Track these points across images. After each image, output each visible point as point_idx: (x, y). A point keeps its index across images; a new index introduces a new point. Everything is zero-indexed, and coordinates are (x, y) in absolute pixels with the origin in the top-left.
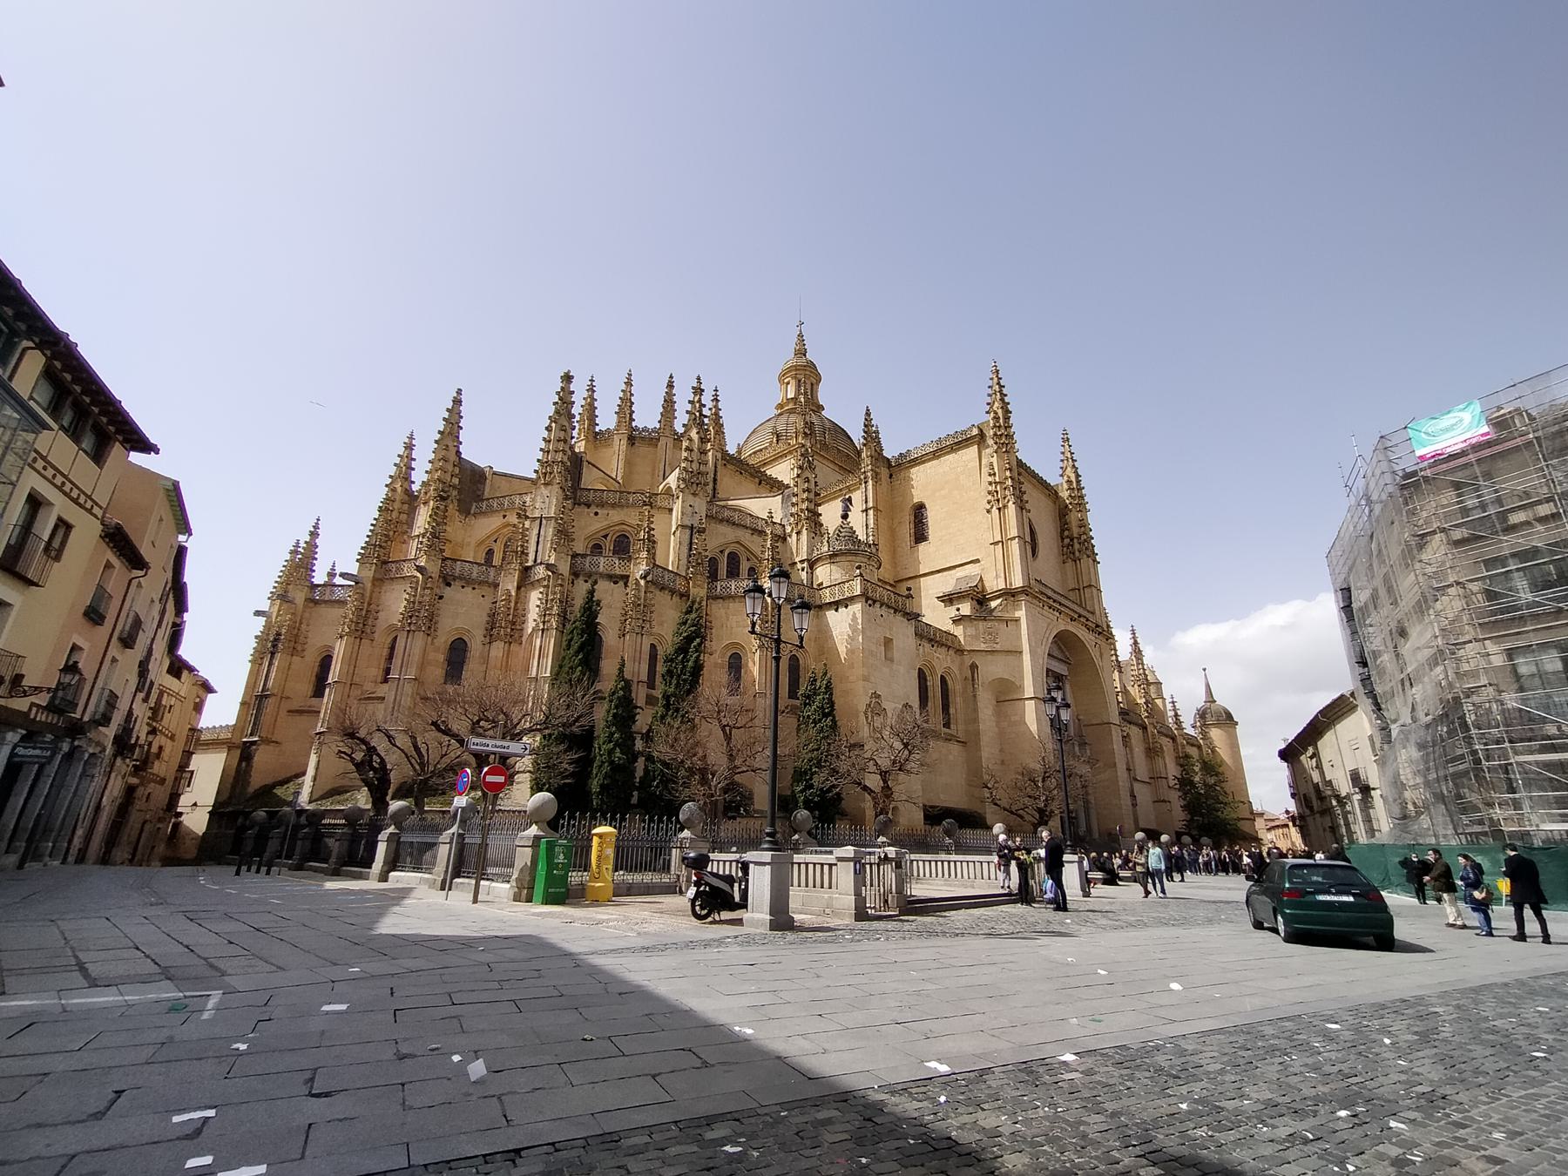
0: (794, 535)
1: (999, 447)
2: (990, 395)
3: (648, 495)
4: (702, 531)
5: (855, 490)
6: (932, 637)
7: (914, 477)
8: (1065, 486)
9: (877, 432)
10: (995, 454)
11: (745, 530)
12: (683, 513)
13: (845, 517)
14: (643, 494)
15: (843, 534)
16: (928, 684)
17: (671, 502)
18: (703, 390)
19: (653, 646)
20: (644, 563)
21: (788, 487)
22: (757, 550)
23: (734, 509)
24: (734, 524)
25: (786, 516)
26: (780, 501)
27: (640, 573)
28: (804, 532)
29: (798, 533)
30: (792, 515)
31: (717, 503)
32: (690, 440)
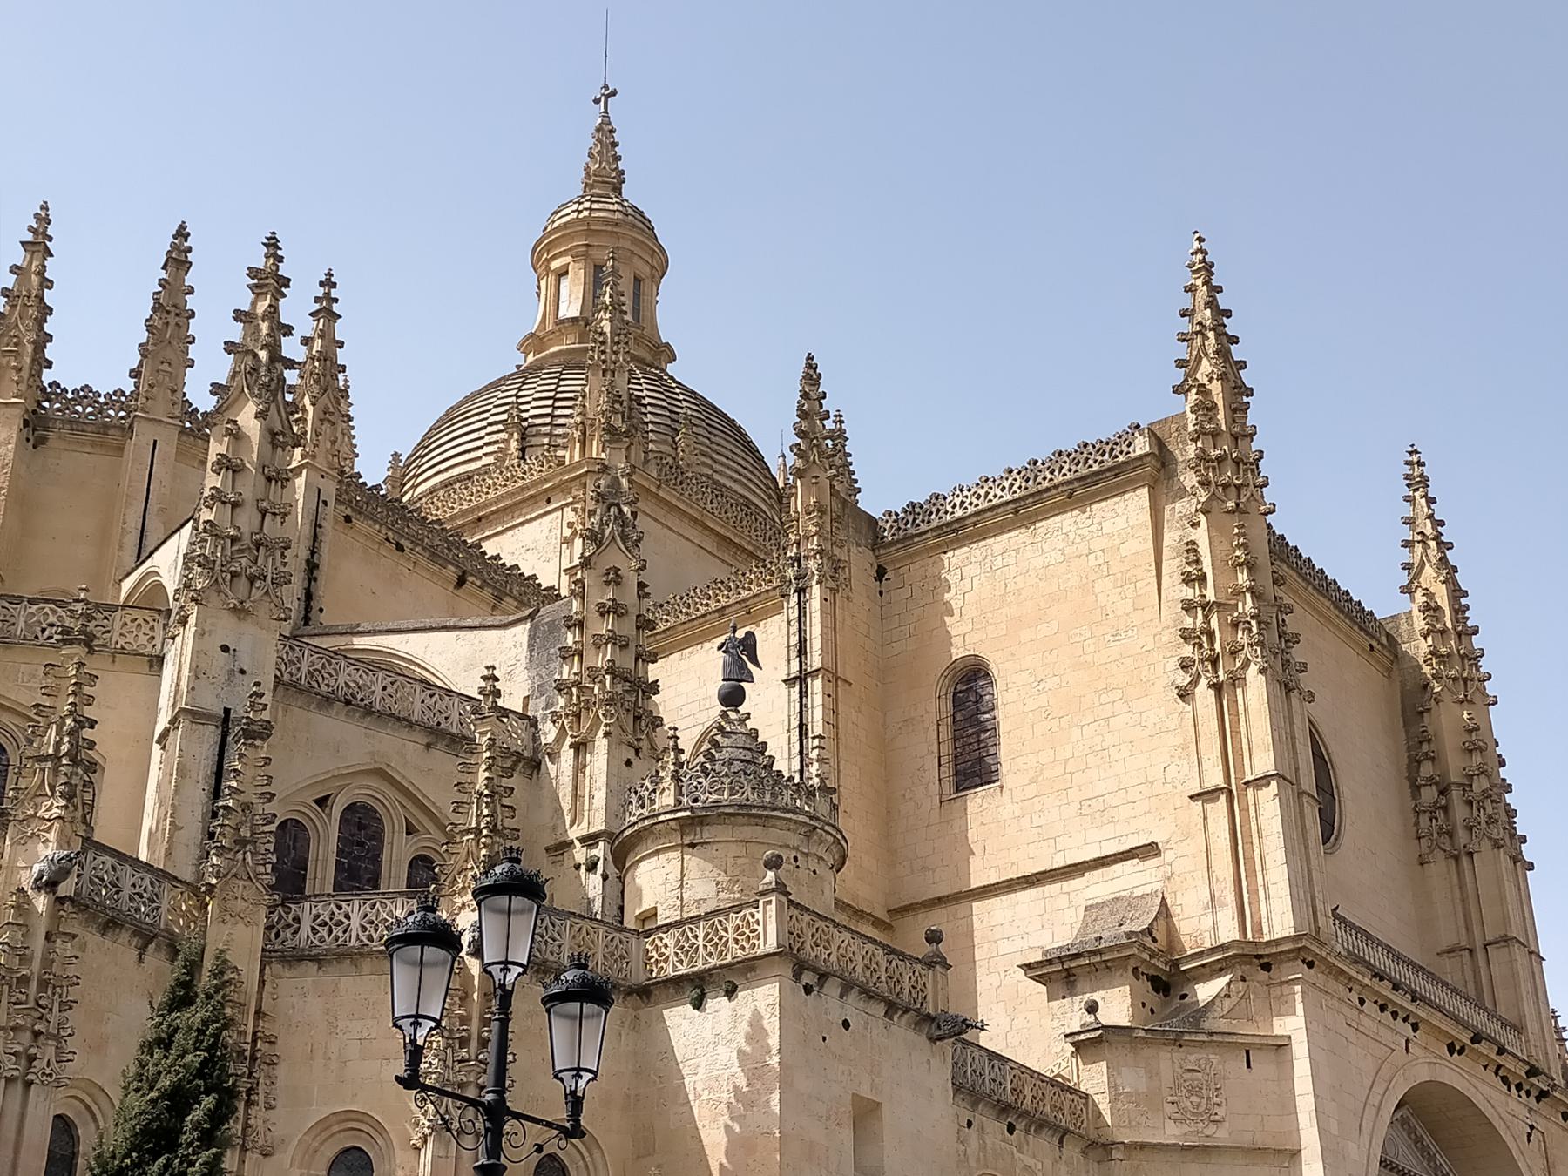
0: (567, 754)
1: (1213, 497)
2: (1183, 338)
3: (79, 608)
4: (258, 733)
5: (767, 614)
7: (952, 579)
8: (1420, 623)
9: (839, 436)
10: (1202, 518)
11: (404, 733)
12: (196, 672)
13: (732, 697)
14: (62, 604)
15: (725, 754)
17: (159, 633)
18: (286, 282)
19: (63, 1127)
20: (52, 836)
21: (552, 595)
22: (440, 798)
23: (375, 663)
24: (368, 711)
25: (540, 690)
26: (525, 639)
27: (37, 868)
28: (601, 743)
29: (580, 747)
30: (561, 687)
31: (316, 641)
32: (236, 435)
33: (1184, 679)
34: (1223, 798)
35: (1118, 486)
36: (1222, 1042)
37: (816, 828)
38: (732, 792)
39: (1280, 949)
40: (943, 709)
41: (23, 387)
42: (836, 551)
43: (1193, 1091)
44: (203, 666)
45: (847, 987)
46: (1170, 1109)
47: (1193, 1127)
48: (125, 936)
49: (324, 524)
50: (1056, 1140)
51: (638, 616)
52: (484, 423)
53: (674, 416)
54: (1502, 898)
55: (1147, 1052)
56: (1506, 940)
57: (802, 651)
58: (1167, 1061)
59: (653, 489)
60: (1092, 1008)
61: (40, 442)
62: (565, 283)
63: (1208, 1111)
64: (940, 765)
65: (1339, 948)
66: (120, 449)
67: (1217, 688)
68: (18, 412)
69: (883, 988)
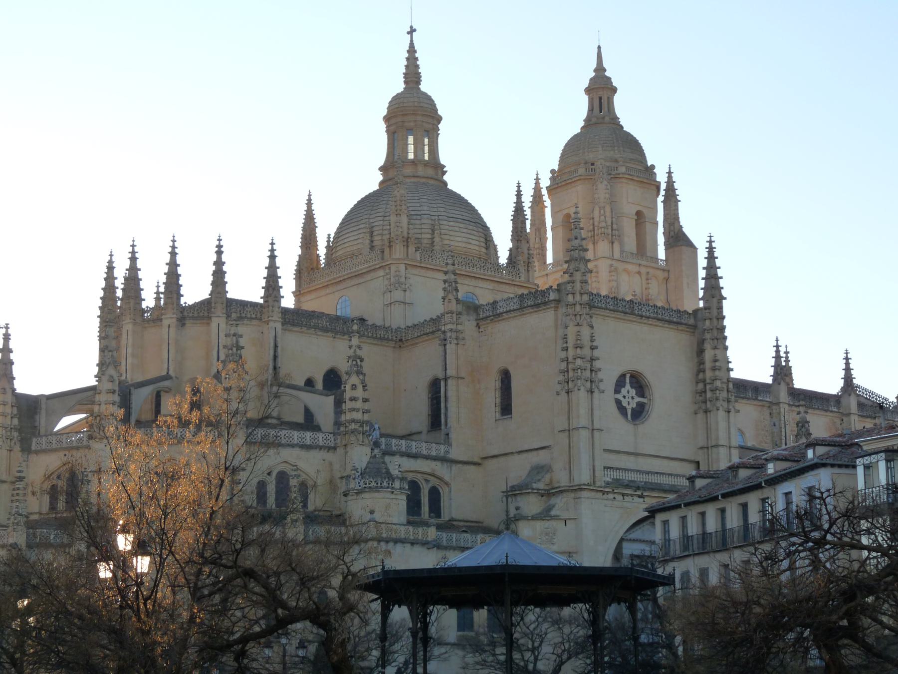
26: (333, 400)
33: (559, 388)
34: (567, 433)
36: (557, 518)
38: (369, 484)
40: (497, 385)
41: (175, 311)
42: (459, 327)
43: (547, 534)
51: (363, 399)
52: (358, 227)
53: (433, 218)
54: (717, 430)
55: (533, 523)
56: (717, 446)
57: (446, 369)
58: (539, 525)
59: (418, 265)
60: (517, 508)
61: (183, 325)
62: (396, 135)
65: (608, 479)
66: (208, 324)
67: (568, 392)
68: (174, 320)
69: (412, 537)
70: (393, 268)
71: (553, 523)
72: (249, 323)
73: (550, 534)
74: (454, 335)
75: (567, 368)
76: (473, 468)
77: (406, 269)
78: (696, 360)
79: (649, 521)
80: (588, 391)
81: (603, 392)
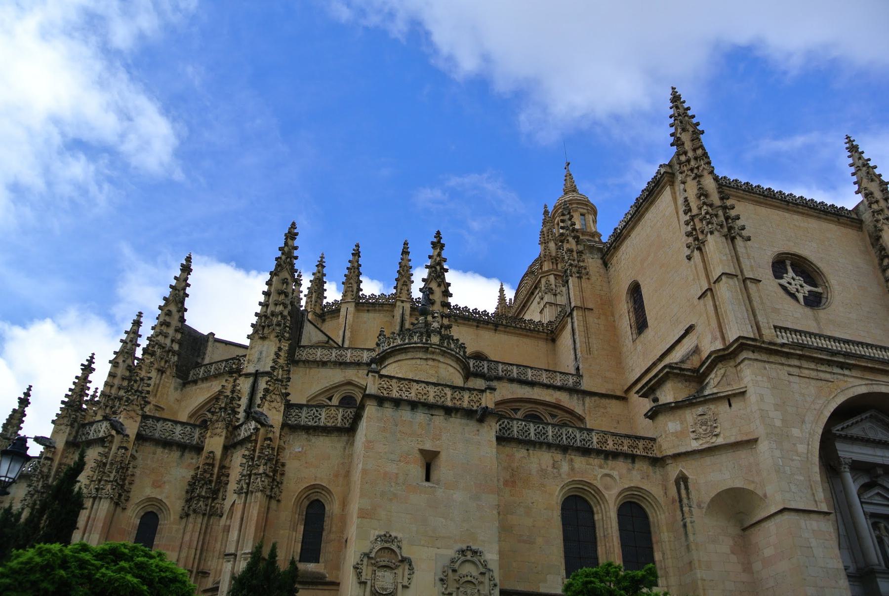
6: (595, 445)
16: (596, 517)
34: (709, 293)
35: (660, 191)
36: (715, 399)
37: (428, 348)
39: (732, 349)
42: (581, 264)
43: (704, 423)
44: (251, 358)
45: (414, 405)
46: (693, 435)
47: (705, 441)
48: (174, 448)
49: (406, 317)
50: (629, 461)
55: (680, 412)
58: (690, 416)
60: (656, 400)
63: (711, 432)
64: (631, 328)
67: (699, 249)
69: (449, 404)
70: (543, 281)
71: (712, 407)
72: (381, 308)
73: (709, 423)
74: (574, 270)
75: (694, 224)
76: (614, 402)
77: (556, 278)
78: (873, 252)
79: (868, 415)
80: (725, 236)
81: (749, 239)
